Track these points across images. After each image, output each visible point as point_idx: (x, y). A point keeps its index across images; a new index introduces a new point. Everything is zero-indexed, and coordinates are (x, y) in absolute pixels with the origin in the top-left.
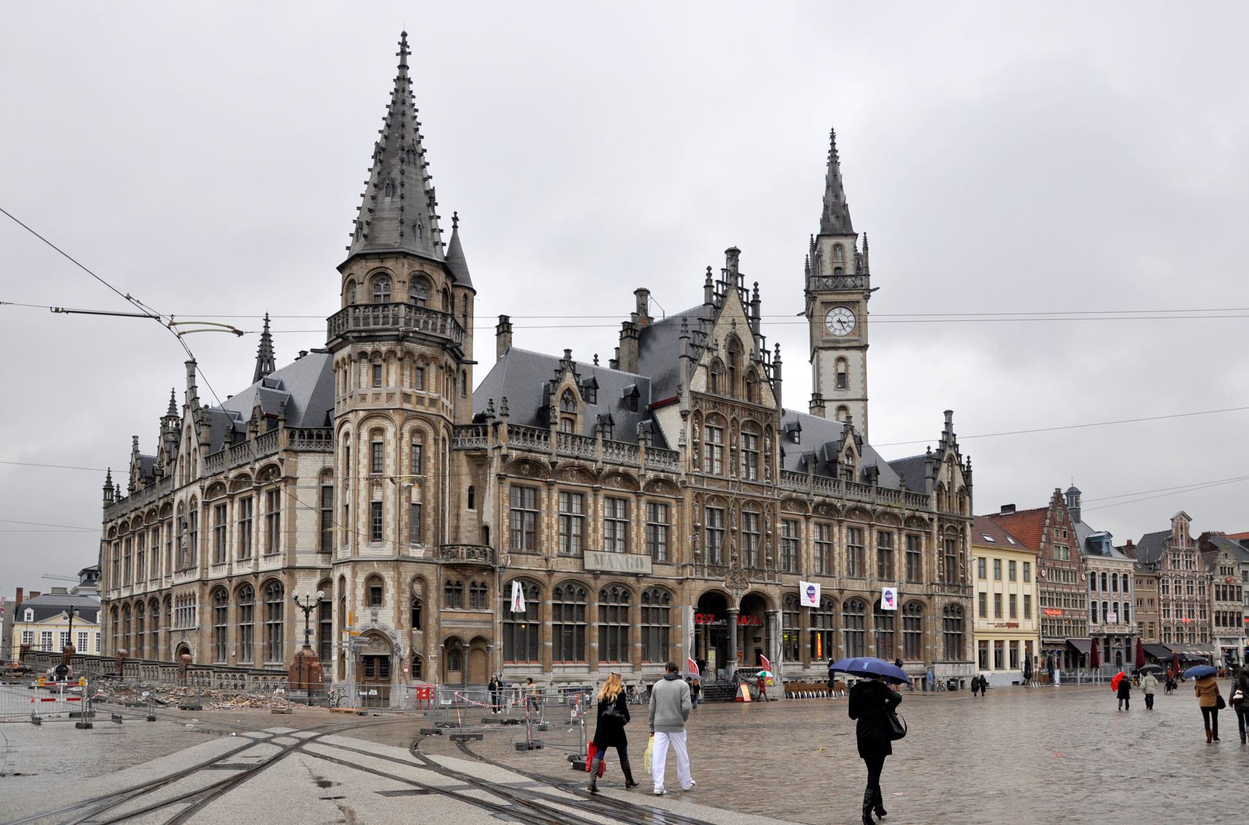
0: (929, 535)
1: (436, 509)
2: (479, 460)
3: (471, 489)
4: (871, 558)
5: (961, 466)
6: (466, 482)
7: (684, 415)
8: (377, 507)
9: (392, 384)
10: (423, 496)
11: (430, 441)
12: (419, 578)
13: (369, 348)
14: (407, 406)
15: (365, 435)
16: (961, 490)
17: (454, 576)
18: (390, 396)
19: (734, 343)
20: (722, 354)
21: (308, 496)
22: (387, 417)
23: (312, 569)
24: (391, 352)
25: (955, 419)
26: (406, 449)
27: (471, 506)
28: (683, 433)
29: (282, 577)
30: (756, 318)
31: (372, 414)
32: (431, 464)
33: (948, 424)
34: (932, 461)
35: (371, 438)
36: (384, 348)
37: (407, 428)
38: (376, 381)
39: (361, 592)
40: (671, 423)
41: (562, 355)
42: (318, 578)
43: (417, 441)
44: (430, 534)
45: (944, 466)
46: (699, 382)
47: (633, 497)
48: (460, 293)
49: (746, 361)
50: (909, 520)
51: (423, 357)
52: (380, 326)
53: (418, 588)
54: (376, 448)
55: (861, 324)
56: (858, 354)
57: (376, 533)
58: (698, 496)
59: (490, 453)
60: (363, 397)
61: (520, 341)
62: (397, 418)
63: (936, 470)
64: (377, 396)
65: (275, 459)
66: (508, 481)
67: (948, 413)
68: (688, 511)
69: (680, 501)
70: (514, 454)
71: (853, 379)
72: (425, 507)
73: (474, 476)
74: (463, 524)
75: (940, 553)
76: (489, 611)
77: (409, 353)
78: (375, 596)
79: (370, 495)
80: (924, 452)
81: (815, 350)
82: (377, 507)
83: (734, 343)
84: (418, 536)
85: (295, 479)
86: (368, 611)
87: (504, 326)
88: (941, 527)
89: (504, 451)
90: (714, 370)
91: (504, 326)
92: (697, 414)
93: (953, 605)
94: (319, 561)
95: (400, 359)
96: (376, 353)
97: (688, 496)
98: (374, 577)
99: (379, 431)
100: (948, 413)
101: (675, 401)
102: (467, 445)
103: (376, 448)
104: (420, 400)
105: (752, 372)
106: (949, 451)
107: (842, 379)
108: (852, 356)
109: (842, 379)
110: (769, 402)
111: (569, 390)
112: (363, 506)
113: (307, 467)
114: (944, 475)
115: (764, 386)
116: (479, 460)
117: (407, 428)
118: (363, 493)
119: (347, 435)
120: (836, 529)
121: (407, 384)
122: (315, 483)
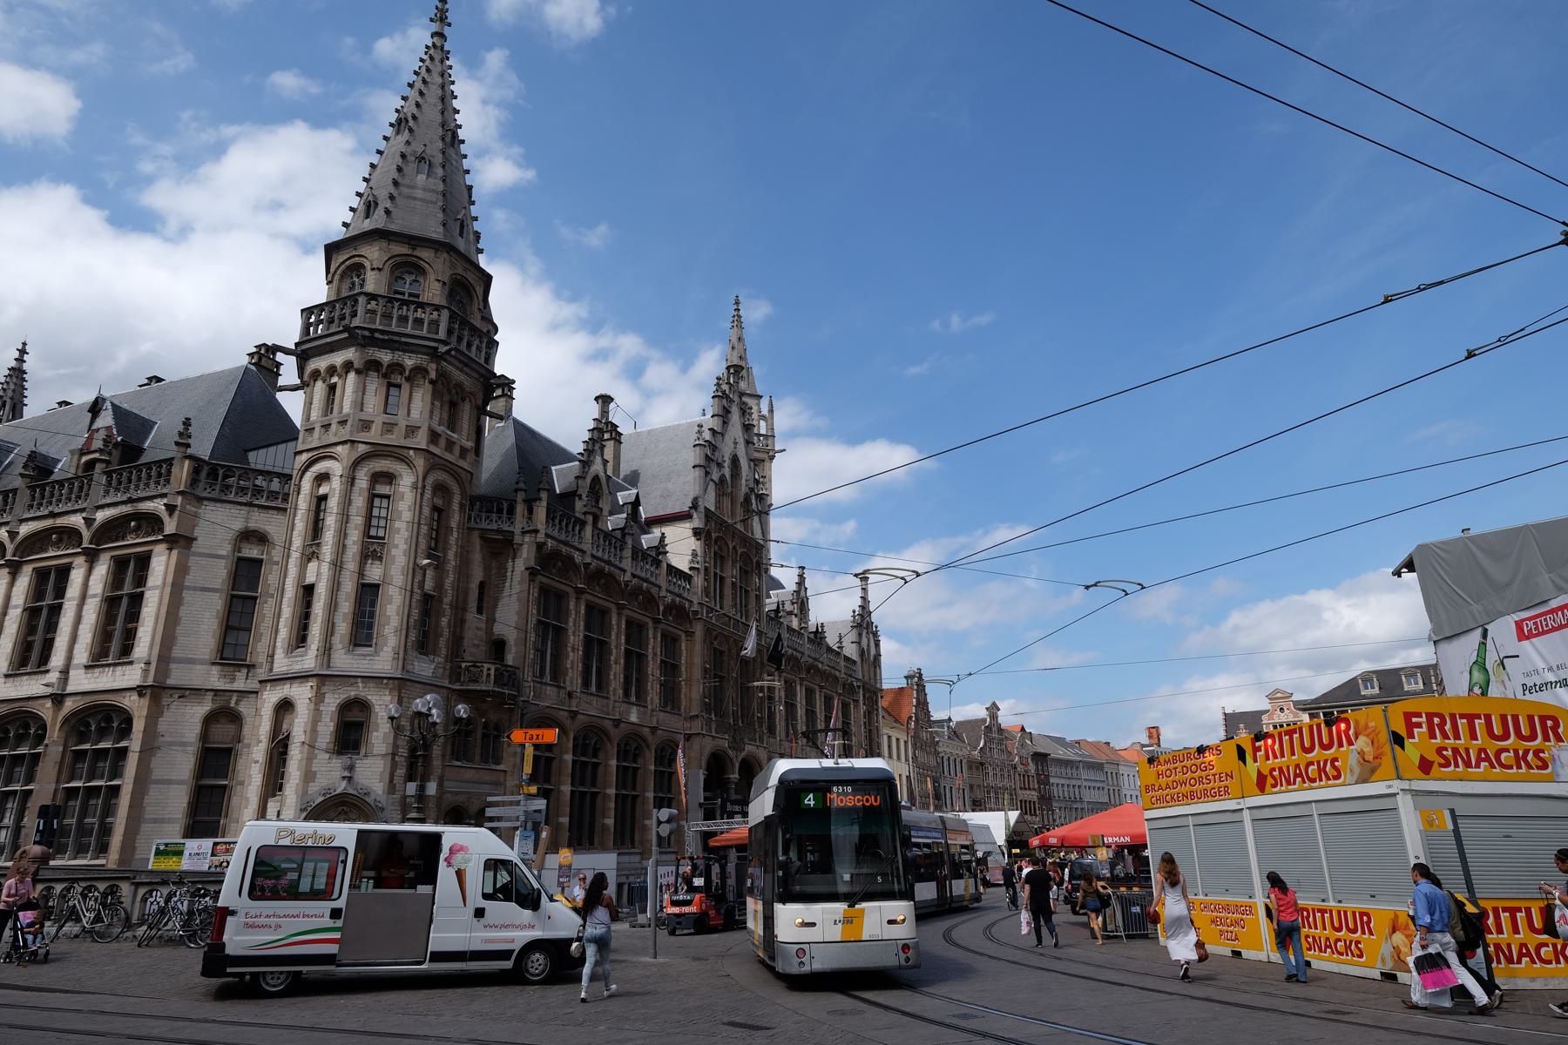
2: (500, 548)
3: (482, 585)
8: (368, 593)
9: (415, 414)
10: (439, 585)
11: (456, 506)
13: (385, 357)
14: (433, 449)
15: (362, 482)
18: (412, 430)
21: (213, 573)
22: (409, 464)
23: (197, 692)
24: (419, 371)
27: (480, 611)
29: (132, 702)
31: (378, 451)
32: (453, 539)
35: (372, 486)
36: (409, 362)
37: (430, 480)
42: (201, 709)
43: (439, 502)
52: (409, 330)
57: (363, 632)
59: (517, 539)
60: (366, 425)
62: (420, 463)
64: (389, 427)
65: (158, 506)
72: (441, 602)
73: (487, 569)
76: (501, 767)
79: (361, 574)
85: (190, 540)
89: (541, 537)
94: (214, 678)
96: (396, 367)
99: (389, 478)
102: (484, 525)
104: (450, 445)
112: (349, 586)
117: (430, 480)
118: (351, 565)
119: (323, 478)
121: (436, 418)
122: (225, 550)
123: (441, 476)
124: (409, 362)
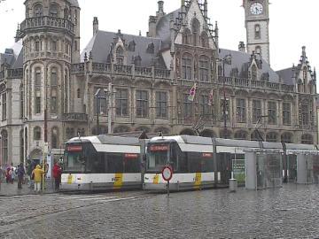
0: (294, 104)
1: (62, 99)
3: (79, 90)
4: (265, 112)
5: (311, 71)
6: (76, 87)
7: (172, 54)
8: (38, 99)
9: (43, 48)
12: (55, 127)
13: (34, 35)
15: (33, 71)
16: (311, 82)
17: (70, 126)
18: (43, 54)
19: (195, 22)
20: (189, 27)
24: (42, 36)
25: (306, 51)
26: (49, 75)
28: (172, 61)
30: (205, 10)
33: (304, 53)
34: (296, 70)
36: (39, 35)
38: (37, 49)
39: (32, 134)
40: (167, 57)
41: (117, 32)
44: (60, 110)
45: (302, 72)
46: (179, 40)
47: (149, 90)
48: (73, 10)
49: (201, 30)
50: (283, 97)
51: (55, 37)
53: (55, 131)
54: (37, 75)
55: (265, 11)
56: (265, 23)
58: (179, 88)
61: (101, 27)
63: (297, 74)
66: (93, 86)
67: (304, 48)
68: (174, 95)
69: (171, 91)
70: (116, 76)
71: (263, 33)
74: (75, 104)
75: (300, 112)
77: (49, 36)
78: (38, 136)
79: (35, 94)
80: (291, 66)
81: (247, 21)
82: (38, 99)
83: (195, 22)
84: (54, 111)
86: (35, 142)
87: (96, 21)
88: (300, 99)
90: (185, 36)
91: (96, 21)
92: (178, 53)
93: (306, 135)
95: (46, 39)
97: (174, 89)
98: (37, 128)
100: (304, 48)
101: (169, 48)
103: (37, 75)
105: (204, 34)
106: (303, 65)
107: (258, 34)
108: (263, 24)
109: (258, 34)
110: (212, 47)
111: (120, 46)
113: (15, 84)
114: (301, 76)
115: (210, 40)
116: (81, 78)
120: (247, 102)
123: (52, 64)
124: (39, 35)
